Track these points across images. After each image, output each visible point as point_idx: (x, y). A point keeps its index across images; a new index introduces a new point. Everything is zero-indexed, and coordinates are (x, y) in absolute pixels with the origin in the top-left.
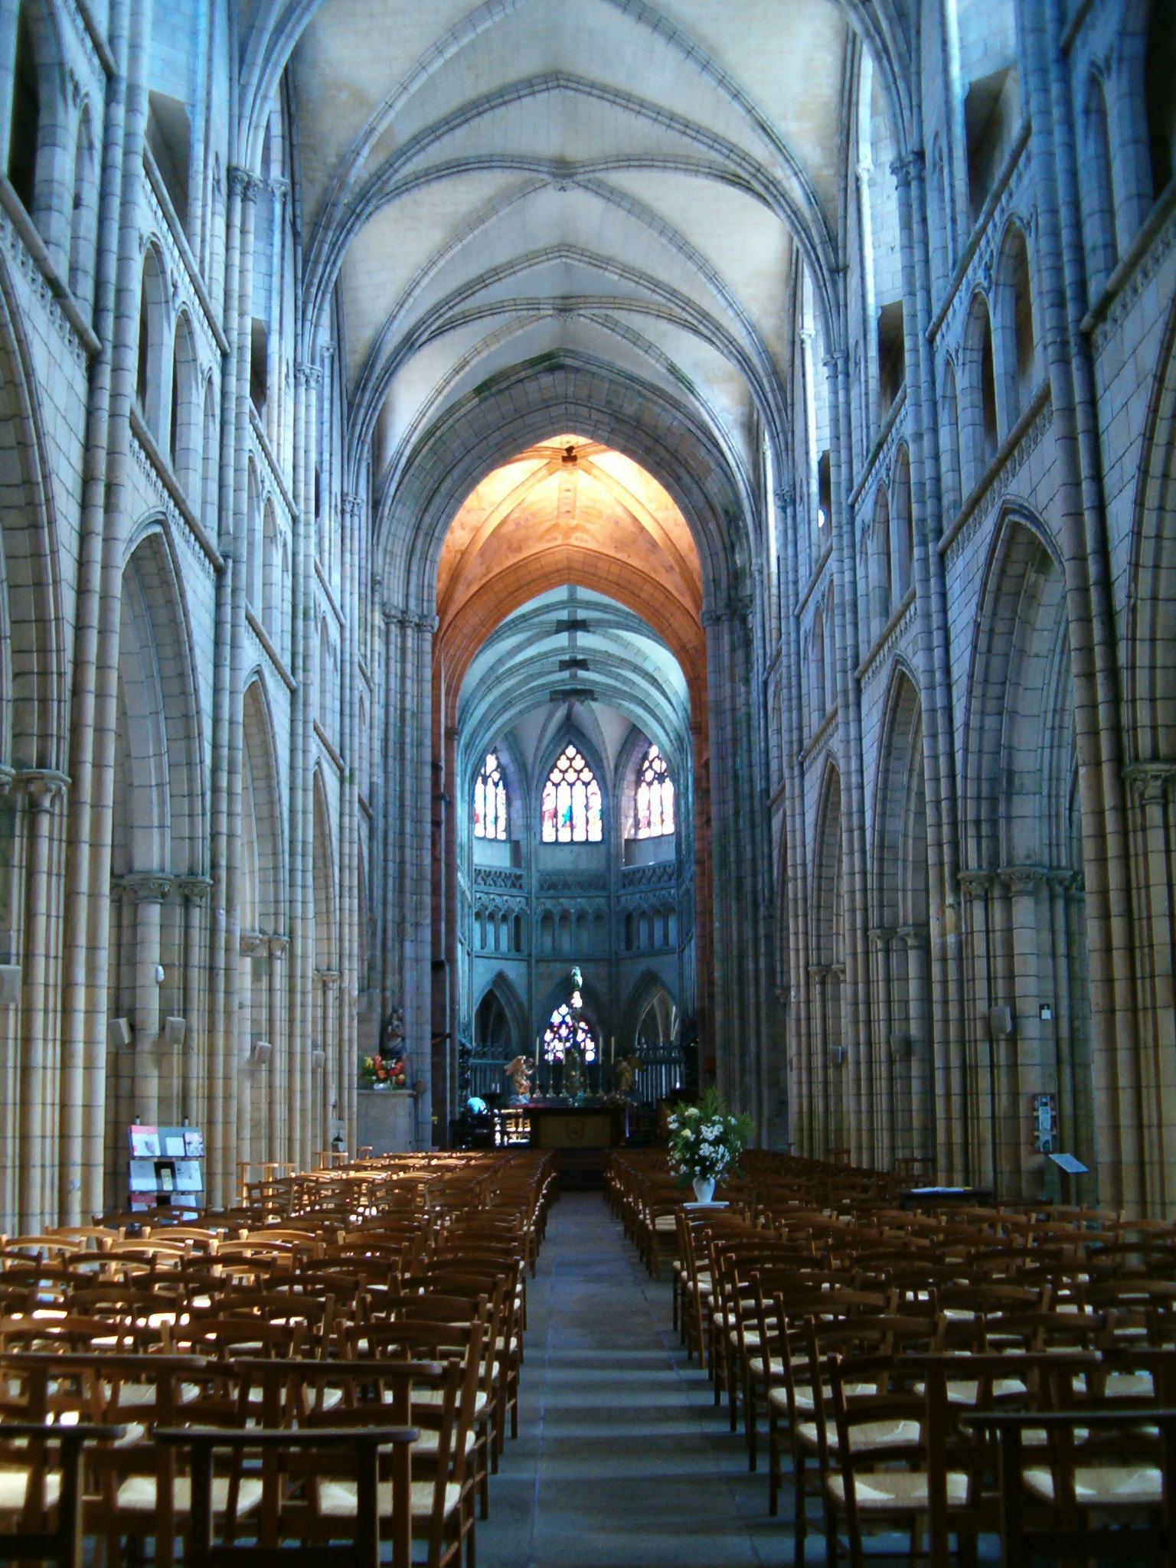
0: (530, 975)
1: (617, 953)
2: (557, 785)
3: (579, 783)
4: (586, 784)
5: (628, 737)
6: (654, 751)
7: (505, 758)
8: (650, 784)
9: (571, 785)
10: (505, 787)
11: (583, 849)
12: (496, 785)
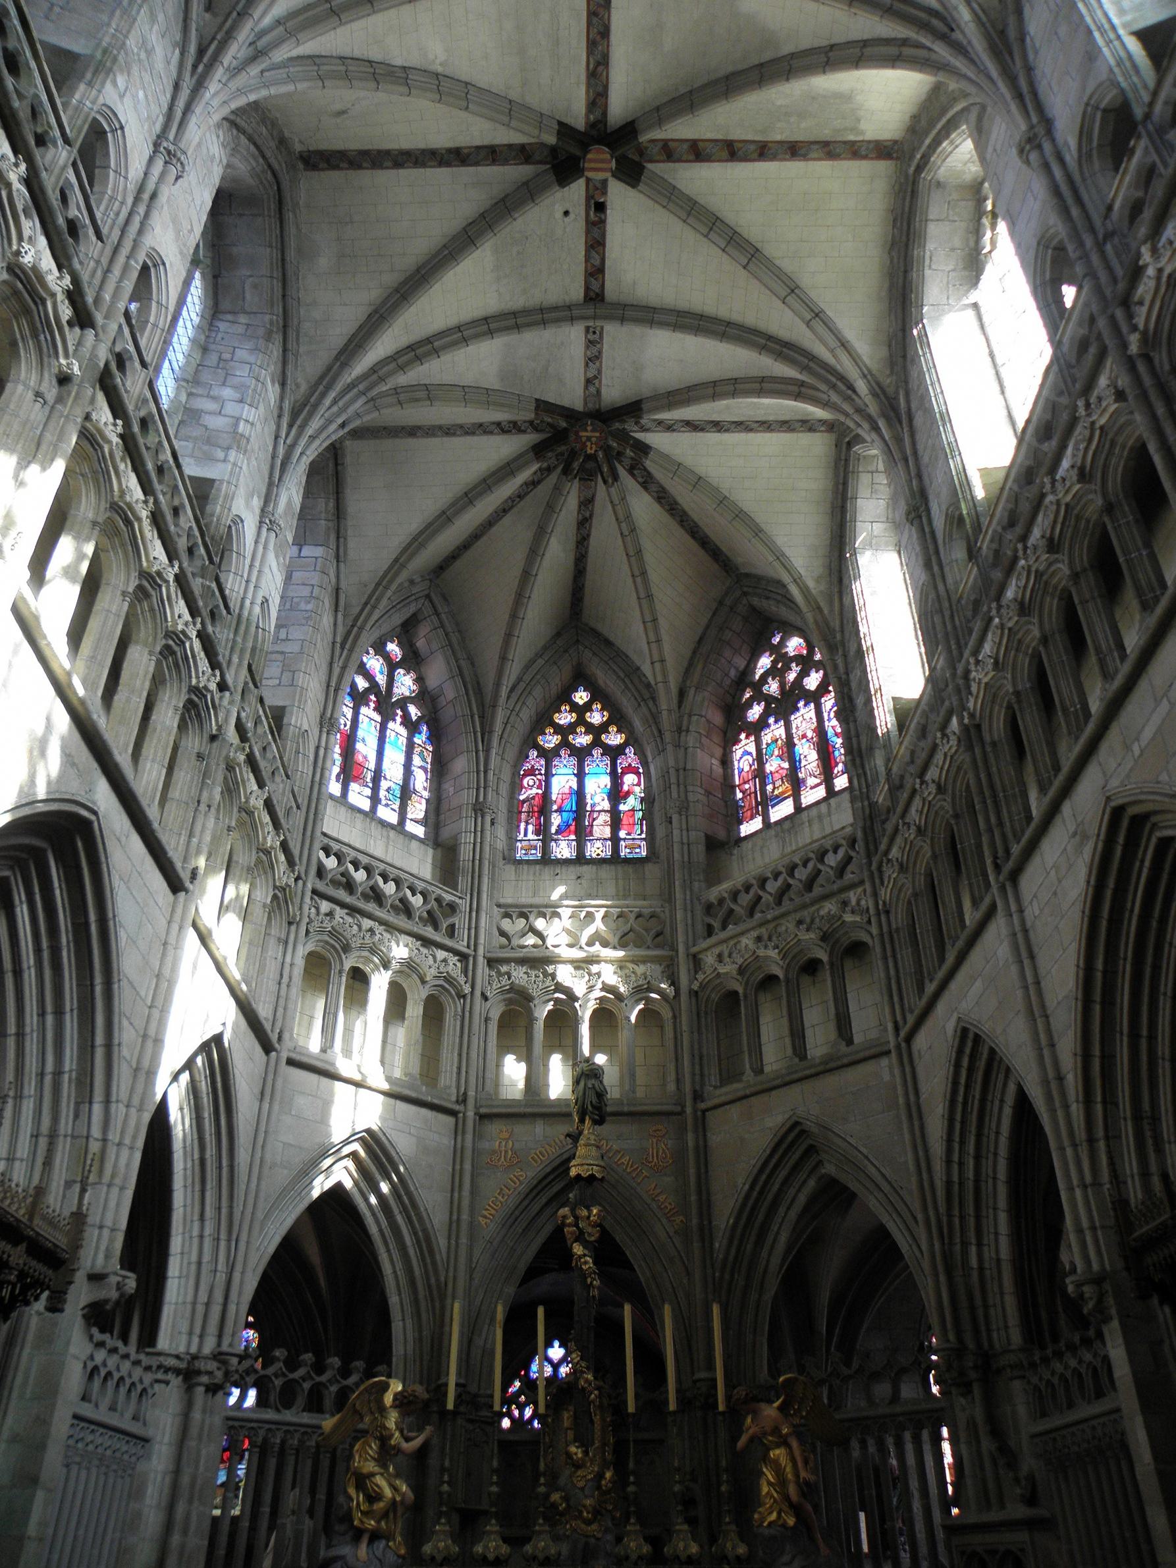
0: (458, 1154)
1: (697, 1097)
2: (549, 756)
3: (597, 752)
4: (614, 753)
5: (707, 627)
6: (765, 662)
7: (438, 672)
8: (757, 729)
9: (581, 755)
10: (435, 737)
11: (606, 872)
12: (412, 727)
